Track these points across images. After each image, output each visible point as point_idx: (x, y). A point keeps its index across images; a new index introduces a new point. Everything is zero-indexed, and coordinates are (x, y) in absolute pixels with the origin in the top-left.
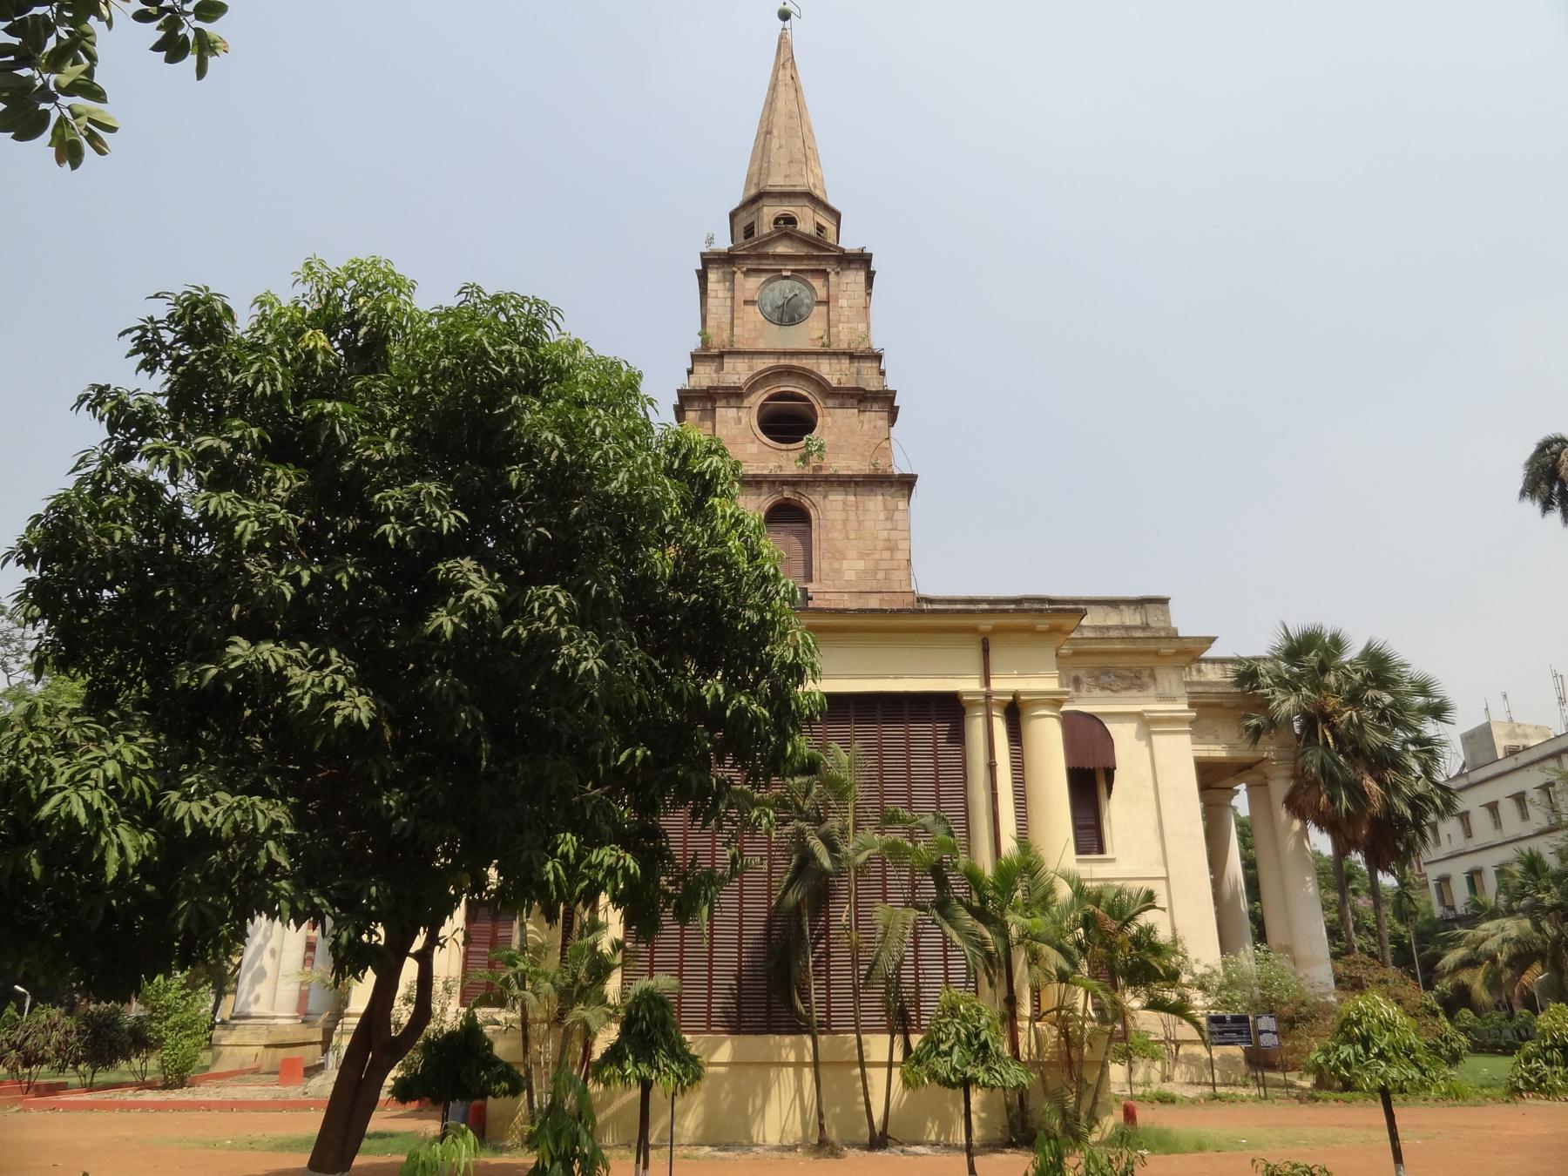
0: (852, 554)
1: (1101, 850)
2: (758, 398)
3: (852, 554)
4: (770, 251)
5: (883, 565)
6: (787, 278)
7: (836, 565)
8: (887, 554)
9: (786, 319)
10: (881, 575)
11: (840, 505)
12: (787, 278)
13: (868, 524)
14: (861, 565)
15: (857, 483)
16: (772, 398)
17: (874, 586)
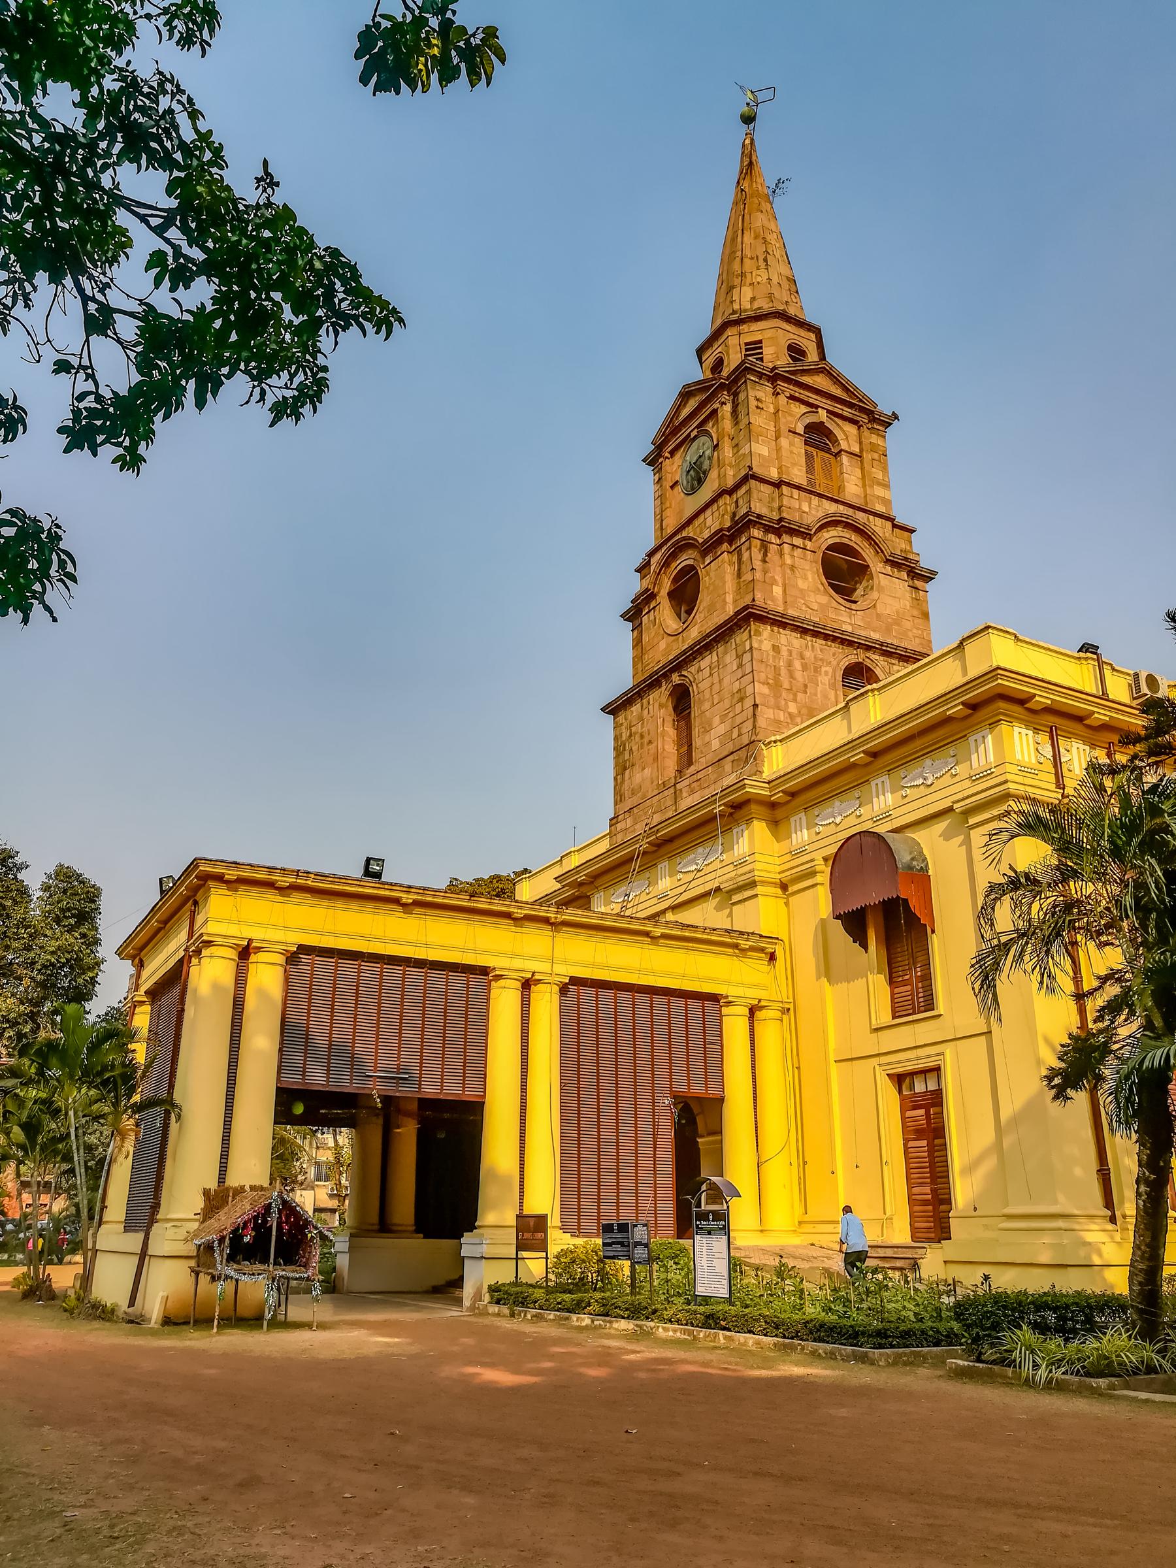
0: (717, 720)
1: (930, 1005)
2: (666, 585)
3: (717, 720)
4: (681, 418)
5: (738, 720)
6: (696, 437)
7: (707, 739)
8: (738, 707)
9: (696, 483)
10: (735, 735)
11: (707, 672)
12: (696, 437)
13: (726, 681)
14: (721, 729)
15: (717, 640)
16: (675, 580)
17: (730, 747)
